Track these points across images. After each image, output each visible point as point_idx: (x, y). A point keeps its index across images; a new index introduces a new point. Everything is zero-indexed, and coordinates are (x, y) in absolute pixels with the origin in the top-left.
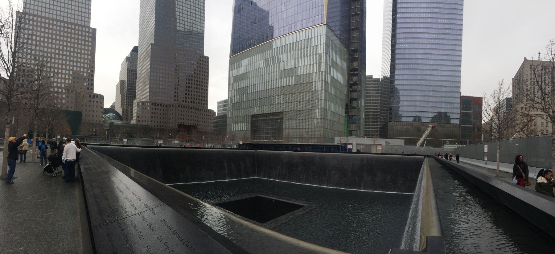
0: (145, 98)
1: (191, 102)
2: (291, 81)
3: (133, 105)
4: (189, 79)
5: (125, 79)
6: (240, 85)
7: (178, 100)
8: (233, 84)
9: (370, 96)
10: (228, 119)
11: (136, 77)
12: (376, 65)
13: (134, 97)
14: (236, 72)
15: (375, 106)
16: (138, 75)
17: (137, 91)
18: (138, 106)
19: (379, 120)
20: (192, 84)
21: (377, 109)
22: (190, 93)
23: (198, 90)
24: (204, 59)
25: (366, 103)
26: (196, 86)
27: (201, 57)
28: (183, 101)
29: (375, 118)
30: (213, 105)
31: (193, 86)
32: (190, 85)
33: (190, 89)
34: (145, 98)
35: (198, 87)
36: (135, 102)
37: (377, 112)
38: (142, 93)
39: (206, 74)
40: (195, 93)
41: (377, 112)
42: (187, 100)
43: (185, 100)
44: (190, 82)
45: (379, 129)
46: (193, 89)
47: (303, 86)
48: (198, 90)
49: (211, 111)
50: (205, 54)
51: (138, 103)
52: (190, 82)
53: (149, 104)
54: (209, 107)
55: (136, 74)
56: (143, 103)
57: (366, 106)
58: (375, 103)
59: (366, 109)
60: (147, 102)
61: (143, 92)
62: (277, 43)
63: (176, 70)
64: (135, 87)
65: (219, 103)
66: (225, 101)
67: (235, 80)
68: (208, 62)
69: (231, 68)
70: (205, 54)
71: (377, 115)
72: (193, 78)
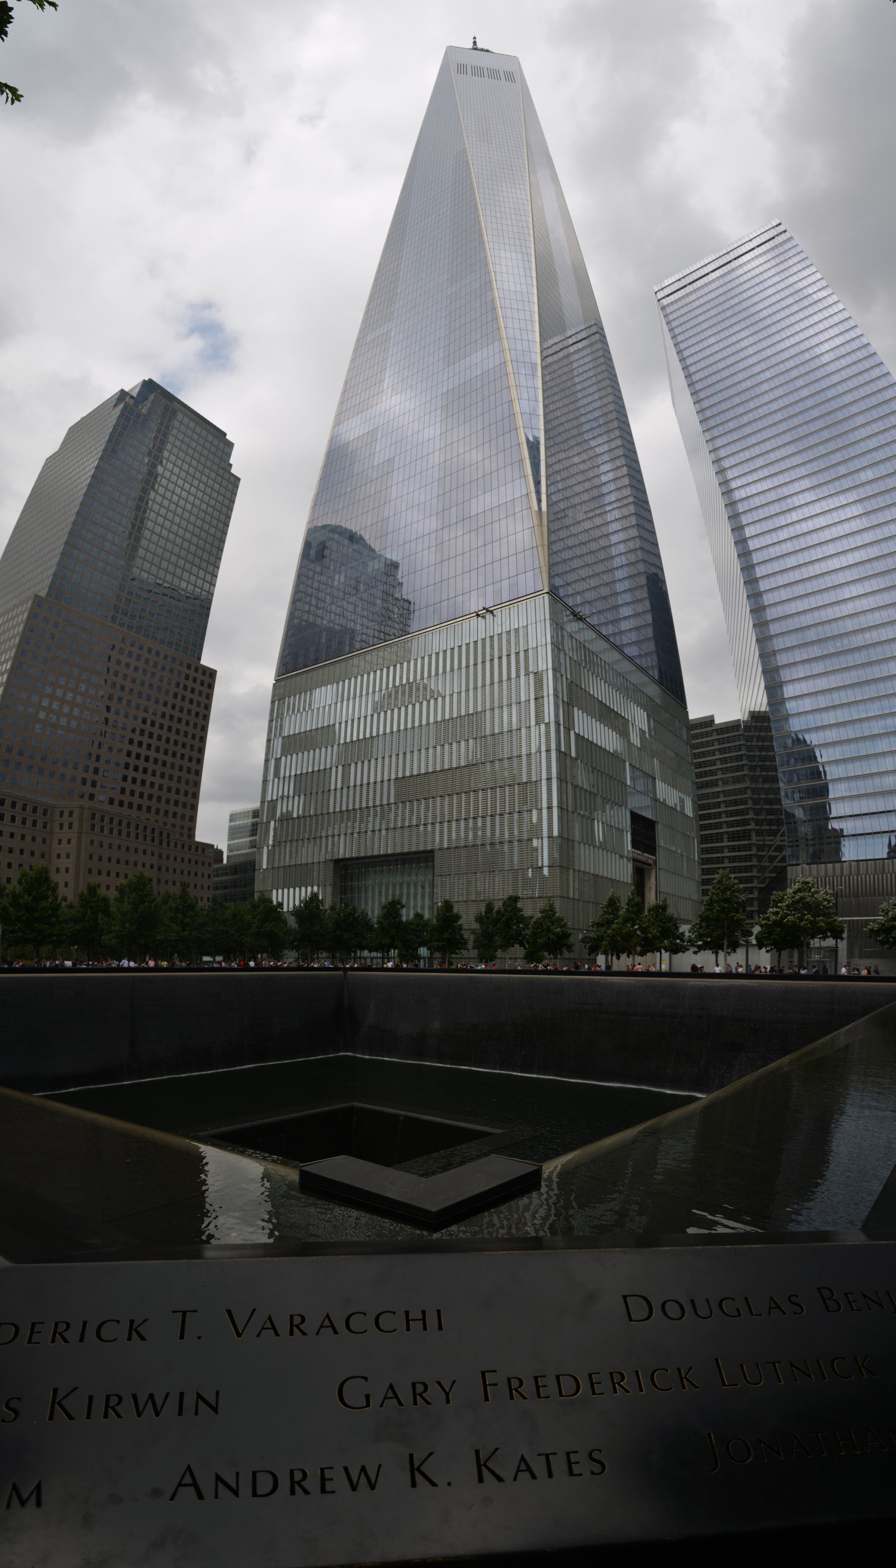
1: (140, 808)
4: (142, 732)
7: (92, 797)
9: (714, 784)
14: (293, 726)
15: (737, 813)
19: (754, 862)
20: (149, 746)
21: (745, 822)
22: (139, 776)
23: (167, 770)
24: (199, 676)
25: (702, 807)
26: (161, 757)
27: (189, 667)
28: (111, 801)
31: (152, 754)
32: (143, 752)
33: (141, 763)
35: (169, 759)
39: (200, 721)
40: (157, 780)
42: (126, 798)
43: (118, 797)
44: (145, 740)
46: (151, 766)
48: (167, 770)
57: (702, 817)
58: (736, 803)
59: (703, 828)
65: (233, 817)
66: (256, 814)
67: (286, 744)
68: (211, 686)
72: (156, 731)
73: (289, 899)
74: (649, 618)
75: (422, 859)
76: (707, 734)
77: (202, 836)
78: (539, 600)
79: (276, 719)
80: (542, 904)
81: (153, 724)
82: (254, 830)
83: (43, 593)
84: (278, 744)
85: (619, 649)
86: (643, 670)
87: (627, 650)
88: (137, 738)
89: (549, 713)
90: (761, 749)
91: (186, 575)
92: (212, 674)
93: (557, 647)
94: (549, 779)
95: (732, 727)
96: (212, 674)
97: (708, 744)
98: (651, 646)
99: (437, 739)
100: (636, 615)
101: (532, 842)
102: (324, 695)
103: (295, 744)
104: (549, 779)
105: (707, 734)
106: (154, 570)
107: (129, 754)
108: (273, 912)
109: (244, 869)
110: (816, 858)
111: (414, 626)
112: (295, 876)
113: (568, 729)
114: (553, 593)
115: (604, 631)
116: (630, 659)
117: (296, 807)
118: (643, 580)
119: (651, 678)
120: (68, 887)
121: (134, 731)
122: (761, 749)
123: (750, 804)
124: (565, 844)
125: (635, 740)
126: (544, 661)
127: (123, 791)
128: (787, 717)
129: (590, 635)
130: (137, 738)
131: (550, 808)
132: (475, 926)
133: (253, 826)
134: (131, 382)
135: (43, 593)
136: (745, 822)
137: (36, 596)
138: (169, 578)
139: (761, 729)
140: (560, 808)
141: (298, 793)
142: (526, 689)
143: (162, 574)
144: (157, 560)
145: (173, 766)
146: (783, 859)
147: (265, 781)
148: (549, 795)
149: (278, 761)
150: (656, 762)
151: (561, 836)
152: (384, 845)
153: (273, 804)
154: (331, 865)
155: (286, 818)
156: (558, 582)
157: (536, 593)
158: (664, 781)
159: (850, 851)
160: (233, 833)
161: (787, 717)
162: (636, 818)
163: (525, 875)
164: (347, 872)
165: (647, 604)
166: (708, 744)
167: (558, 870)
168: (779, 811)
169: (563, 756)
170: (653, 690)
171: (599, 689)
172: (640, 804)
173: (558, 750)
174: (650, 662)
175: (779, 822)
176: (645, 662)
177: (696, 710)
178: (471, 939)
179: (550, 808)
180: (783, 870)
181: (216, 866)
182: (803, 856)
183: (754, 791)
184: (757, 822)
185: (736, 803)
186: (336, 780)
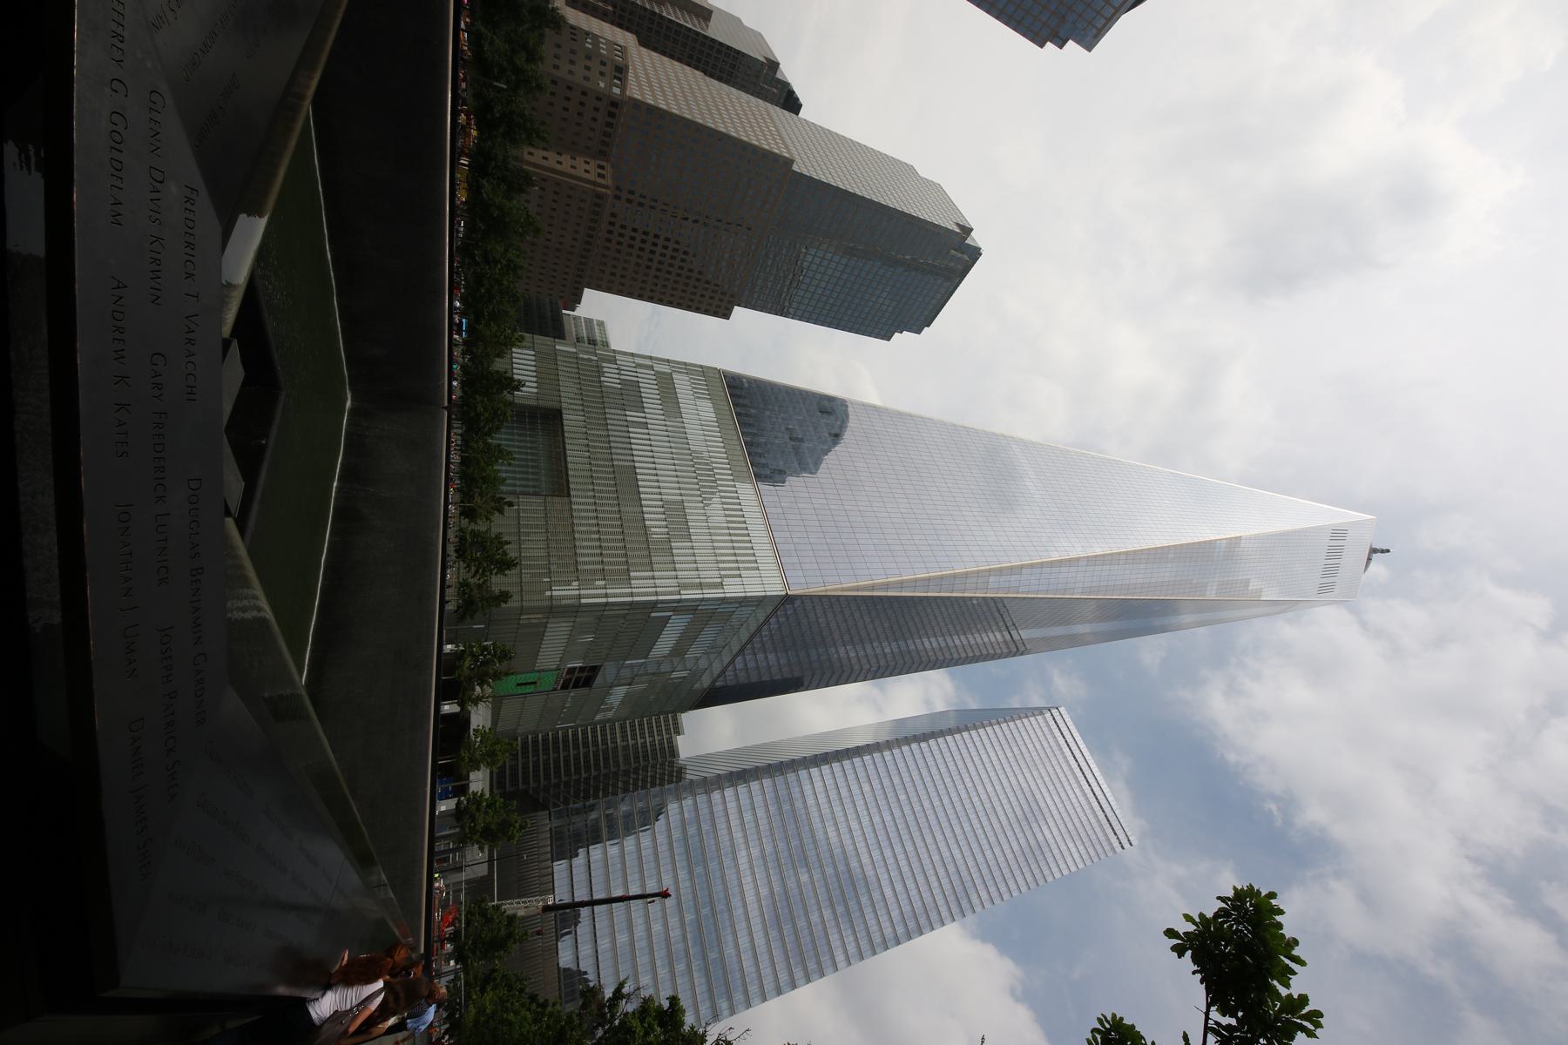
0: (640, 85)
2: (656, 525)
3: (620, 26)
4: (675, 250)
5: (715, 31)
6: (649, 391)
8: (652, 368)
10: (549, 340)
11: (711, 76)
12: (711, 733)
13: (644, 43)
16: (715, 82)
17: (665, 59)
18: (611, 44)
26: (655, 265)
28: (613, 215)
29: (557, 768)
30: (596, 305)
33: (648, 247)
34: (640, 85)
35: (653, 272)
36: (627, 39)
37: (578, 770)
38: (658, 81)
41: (578, 770)
44: (669, 252)
45: (521, 787)
47: (642, 548)
49: (575, 300)
50: (738, 311)
51: (623, 50)
52: (669, 252)
53: (617, 91)
54: (588, 294)
55: (720, 79)
56: (620, 71)
58: (606, 759)
60: (623, 88)
61: (660, 82)
62: (746, 491)
63: (696, 221)
64: (679, 60)
65: (601, 324)
66: (606, 344)
68: (715, 314)
69: (705, 373)
70: (738, 311)
71: (568, 771)
73: (523, 363)
74: (766, 678)
75: (561, 487)
76: (668, 730)
77: (588, 294)
78: (780, 587)
79: (687, 368)
80: (513, 589)
81: (683, 260)
82: (592, 342)
83: (795, 168)
84: (665, 369)
85: (742, 650)
86: (723, 671)
87: (739, 659)
88: (671, 245)
89: (688, 594)
90: (654, 777)
91: (809, 295)
92: (726, 316)
93: (743, 601)
94: (632, 595)
95: (673, 752)
96: (726, 316)
97: (659, 732)
98: (742, 679)
99: (668, 502)
100: (769, 668)
101: (568, 578)
102: (707, 411)
103: (666, 385)
104: (632, 595)
105: (668, 730)
106: (814, 267)
107: (657, 236)
108: (504, 345)
109: (555, 328)
110: (557, 835)
111: (763, 487)
112: (547, 370)
113: (675, 610)
114: (787, 599)
115: (756, 640)
116: (732, 661)
117: (610, 378)
118: (796, 674)
119: (714, 681)
120: (535, 157)
121: (677, 242)
122: (654, 777)
123: (603, 771)
124: (575, 610)
125: (665, 667)
126: (733, 589)
127: (623, 227)
128: (679, 799)
129: (753, 628)
130: (671, 245)
131: (606, 596)
132: (495, 531)
133: (593, 339)
134: (977, 238)
135: (795, 168)
136: (588, 769)
137: (792, 161)
138: (807, 281)
139: (671, 775)
140: (607, 604)
141: (623, 382)
142: (710, 576)
143: (810, 274)
144: (822, 269)
145: (646, 275)
146: (555, 805)
147: (632, 355)
148: (618, 594)
149: (652, 368)
150: (644, 686)
151: (581, 605)
152: (575, 456)
153: (614, 361)
154: (555, 405)
155: (599, 372)
156: (798, 603)
157: (786, 584)
158: (627, 695)
159: (560, 867)
160: (589, 322)
161: (679, 799)
162: (595, 670)
163: (545, 575)
164: (548, 419)
165: (778, 677)
166: (659, 732)
167: (548, 603)
168: (596, 796)
169: (653, 605)
170: (706, 681)
171: (708, 635)
172: (608, 672)
173: (657, 602)
174: (730, 678)
175: (587, 797)
176: (729, 673)
177: (689, 719)
178: (481, 526)
179: (606, 596)
180: (545, 807)
181: (560, 303)
182: (556, 823)
183: (616, 773)
184: (587, 779)
185: (606, 759)
186: (633, 416)
